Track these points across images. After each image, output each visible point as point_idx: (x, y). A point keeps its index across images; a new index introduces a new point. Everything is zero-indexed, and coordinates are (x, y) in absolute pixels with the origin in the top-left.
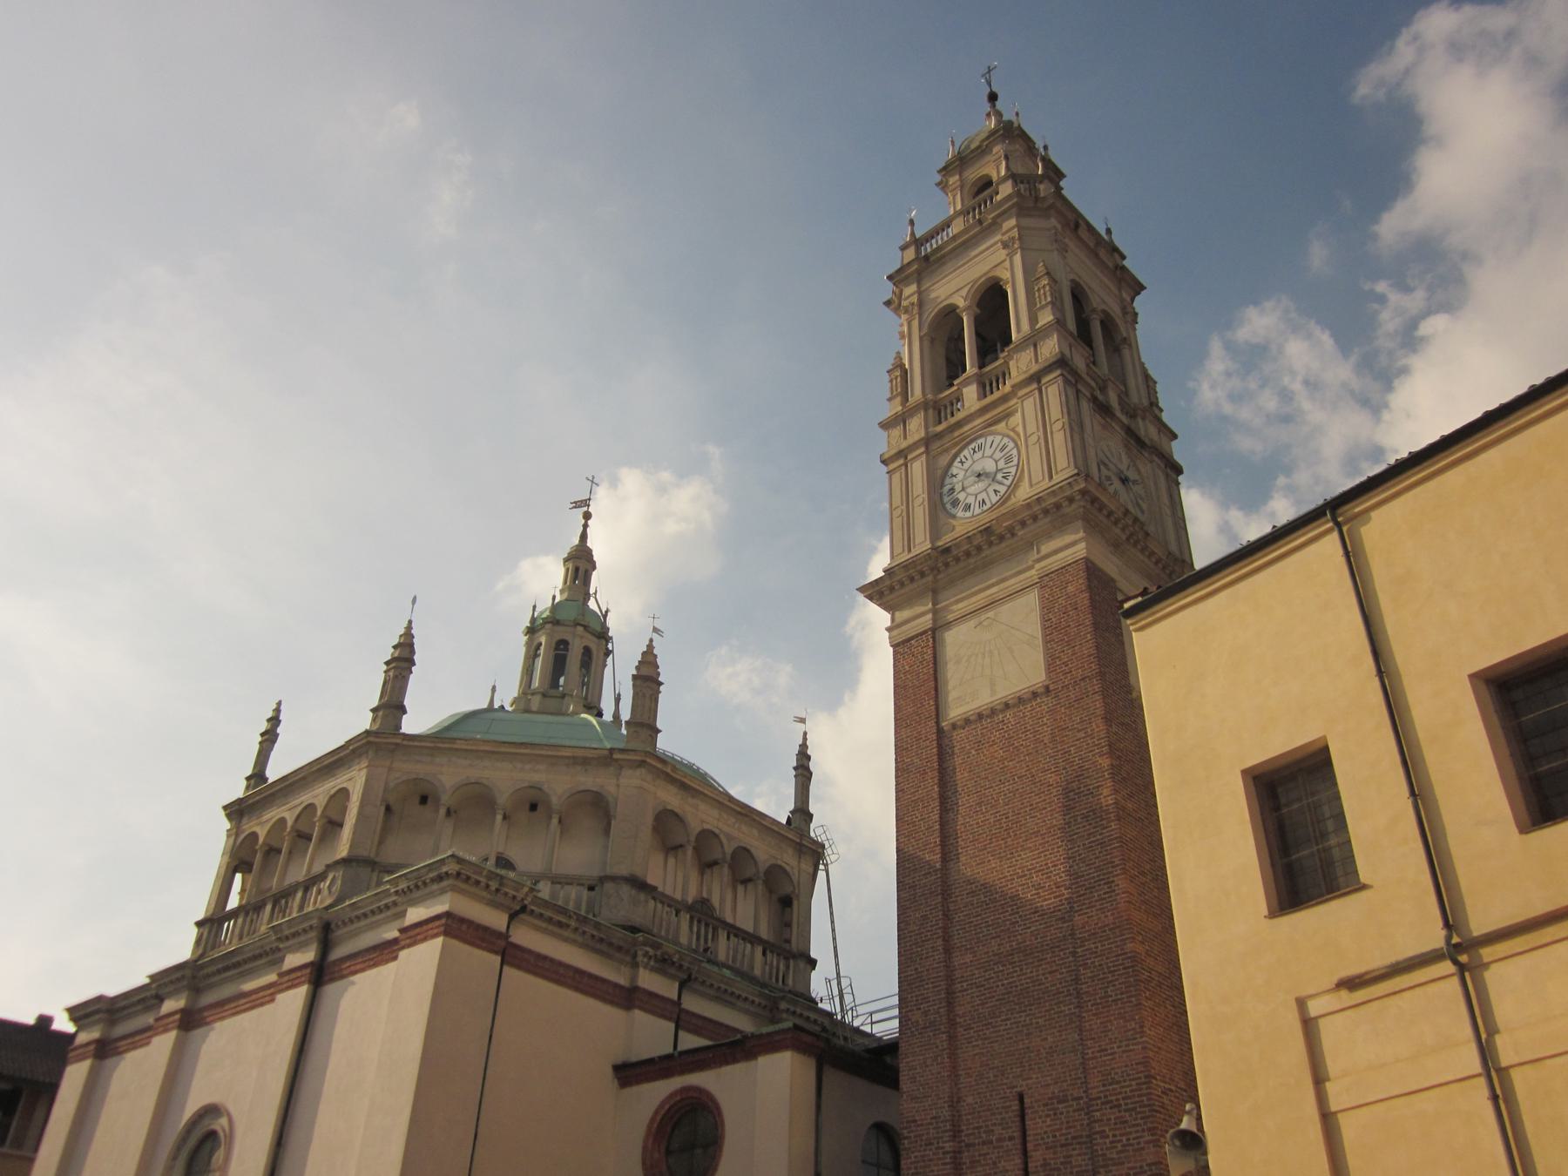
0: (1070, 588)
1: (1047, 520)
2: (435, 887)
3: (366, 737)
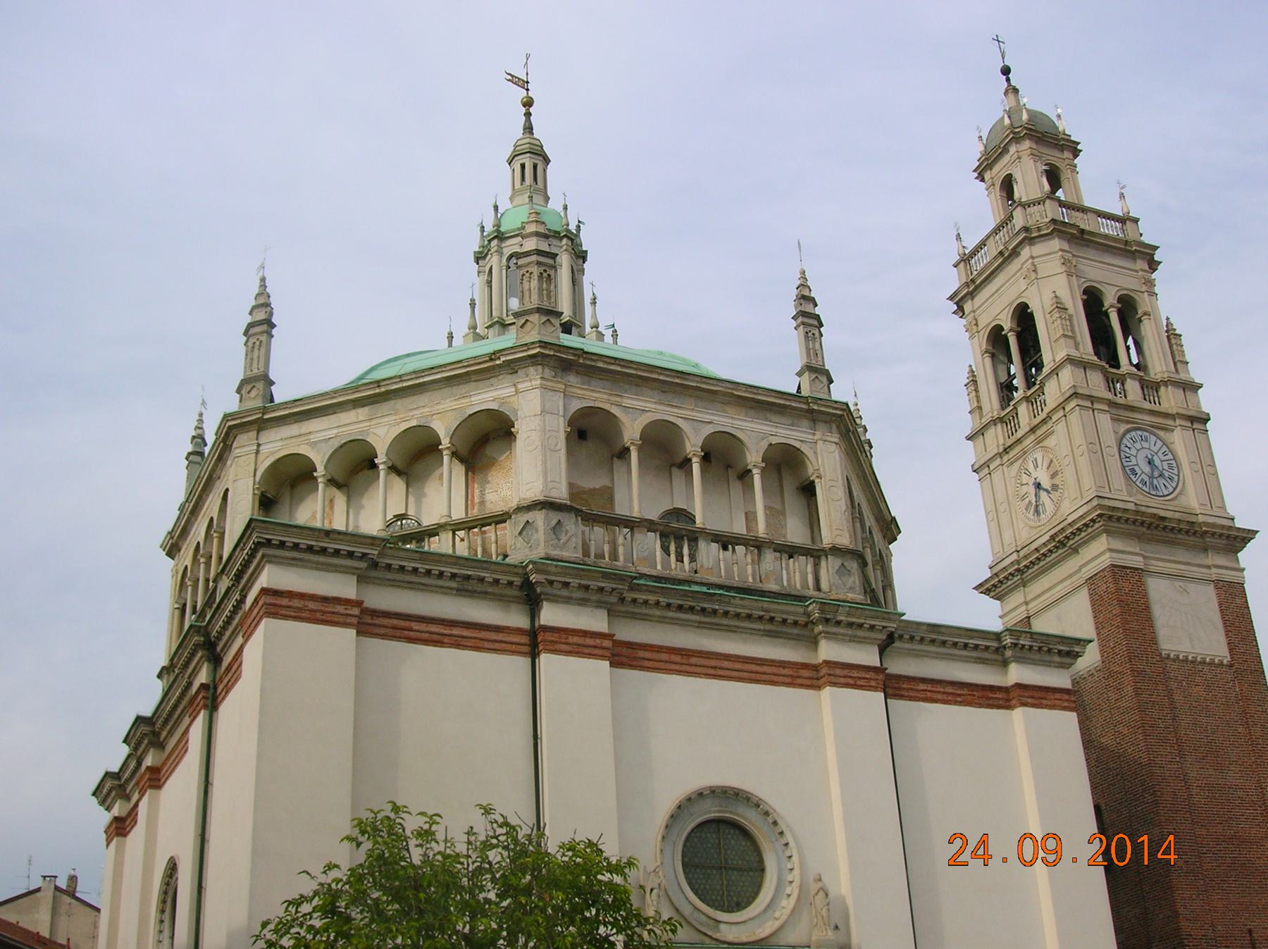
0: (1238, 601)
1: (1224, 542)
2: (1057, 659)
3: (843, 410)
